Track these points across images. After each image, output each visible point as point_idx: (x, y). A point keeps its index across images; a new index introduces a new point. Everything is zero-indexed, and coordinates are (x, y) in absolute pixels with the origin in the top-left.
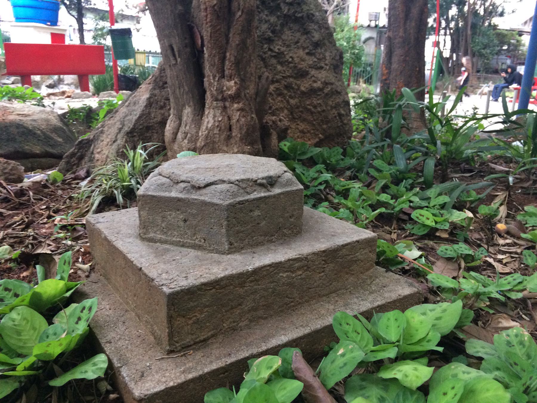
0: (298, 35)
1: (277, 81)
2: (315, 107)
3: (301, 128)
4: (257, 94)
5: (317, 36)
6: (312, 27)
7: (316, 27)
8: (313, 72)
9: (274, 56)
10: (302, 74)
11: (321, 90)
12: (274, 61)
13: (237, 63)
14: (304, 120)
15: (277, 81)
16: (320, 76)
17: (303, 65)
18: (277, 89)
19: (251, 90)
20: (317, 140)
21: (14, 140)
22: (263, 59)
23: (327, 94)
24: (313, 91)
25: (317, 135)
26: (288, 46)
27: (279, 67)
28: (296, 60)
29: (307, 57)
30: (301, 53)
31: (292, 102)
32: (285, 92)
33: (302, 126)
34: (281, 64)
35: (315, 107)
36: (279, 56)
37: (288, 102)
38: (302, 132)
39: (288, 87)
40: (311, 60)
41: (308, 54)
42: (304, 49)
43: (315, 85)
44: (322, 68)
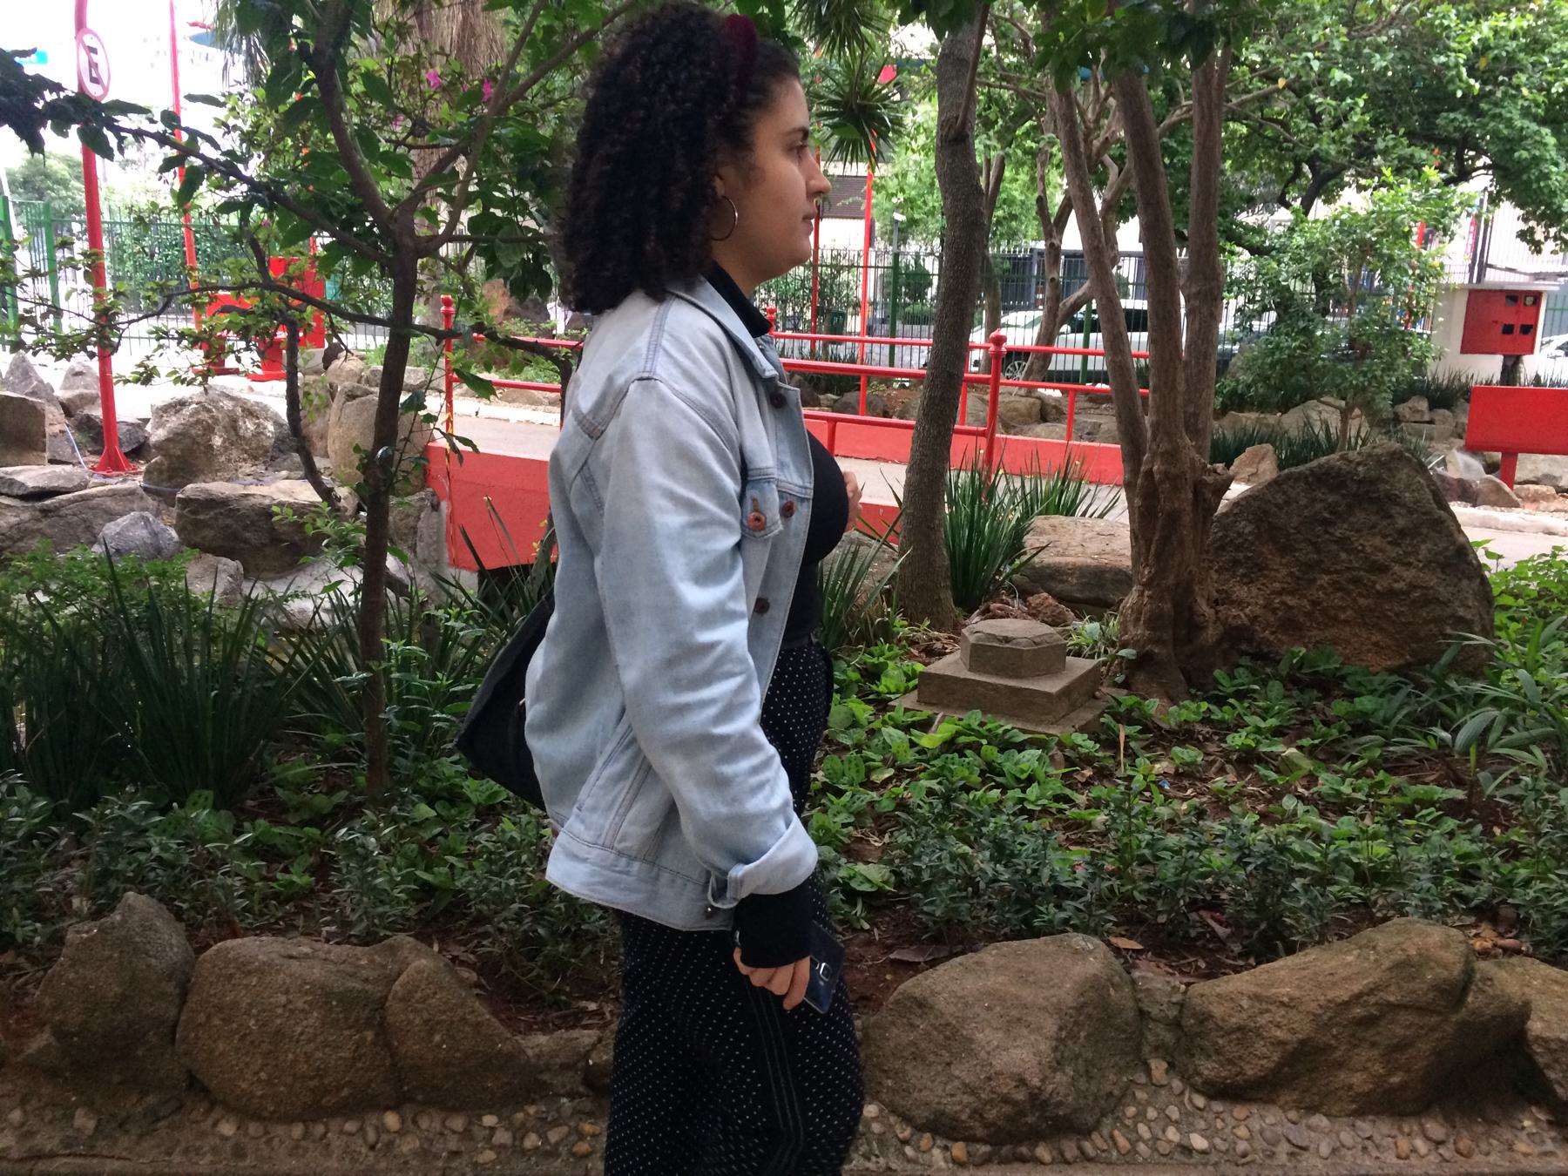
0: (1374, 518)
1: (1336, 572)
2: (1397, 615)
3: (1374, 639)
4: (1177, 585)
5: (1401, 522)
6: (1395, 510)
7: (1403, 511)
8: (1396, 568)
9: (1336, 542)
10: (1382, 569)
11: (1406, 593)
12: (1334, 547)
13: (1158, 556)
14: (1381, 630)
15: (1336, 572)
16: (1405, 574)
17: (1380, 557)
18: (1335, 582)
19: (1171, 580)
20: (1402, 662)
21: (1102, 587)
22: (1314, 544)
23: (1414, 602)
24: (1391, 594)
25: (1402, 655)
26: (1358, 531)
27: (1343, 555)
28: (1369, 550)
29: (1389, 548)
30: (1377, 541)
31: (1362, 601)
32: (1351, 587)
33: (1377, 637)
34: (1346, 551)
35: (1397, 615)
36: (1343, 542)
37: (1354, 600)
38: (1376, 644)
39: (1356, 581)
40: (1394, 552)
41: (1389, 543)
42: (1384, 536)
43: (1396, 586)
44: (1410, 564)
